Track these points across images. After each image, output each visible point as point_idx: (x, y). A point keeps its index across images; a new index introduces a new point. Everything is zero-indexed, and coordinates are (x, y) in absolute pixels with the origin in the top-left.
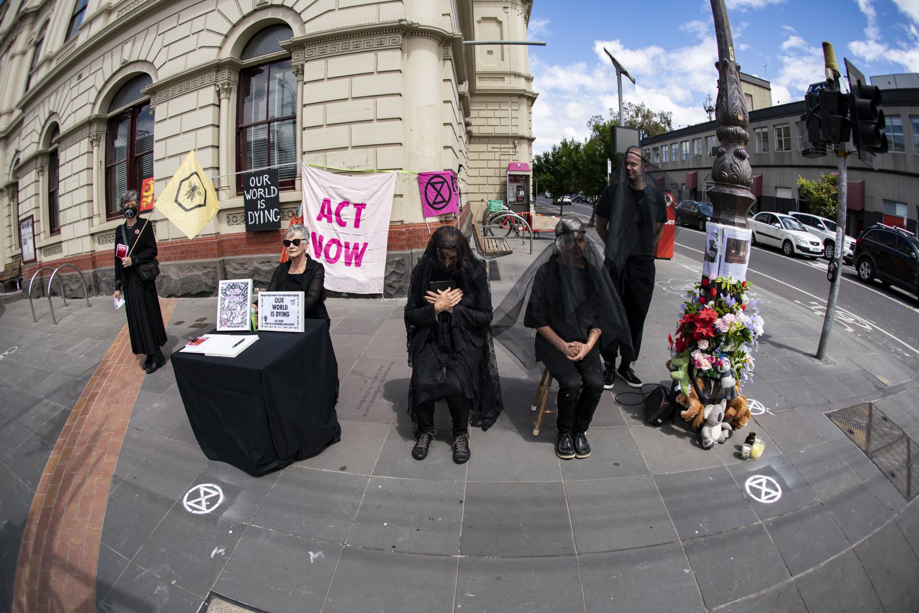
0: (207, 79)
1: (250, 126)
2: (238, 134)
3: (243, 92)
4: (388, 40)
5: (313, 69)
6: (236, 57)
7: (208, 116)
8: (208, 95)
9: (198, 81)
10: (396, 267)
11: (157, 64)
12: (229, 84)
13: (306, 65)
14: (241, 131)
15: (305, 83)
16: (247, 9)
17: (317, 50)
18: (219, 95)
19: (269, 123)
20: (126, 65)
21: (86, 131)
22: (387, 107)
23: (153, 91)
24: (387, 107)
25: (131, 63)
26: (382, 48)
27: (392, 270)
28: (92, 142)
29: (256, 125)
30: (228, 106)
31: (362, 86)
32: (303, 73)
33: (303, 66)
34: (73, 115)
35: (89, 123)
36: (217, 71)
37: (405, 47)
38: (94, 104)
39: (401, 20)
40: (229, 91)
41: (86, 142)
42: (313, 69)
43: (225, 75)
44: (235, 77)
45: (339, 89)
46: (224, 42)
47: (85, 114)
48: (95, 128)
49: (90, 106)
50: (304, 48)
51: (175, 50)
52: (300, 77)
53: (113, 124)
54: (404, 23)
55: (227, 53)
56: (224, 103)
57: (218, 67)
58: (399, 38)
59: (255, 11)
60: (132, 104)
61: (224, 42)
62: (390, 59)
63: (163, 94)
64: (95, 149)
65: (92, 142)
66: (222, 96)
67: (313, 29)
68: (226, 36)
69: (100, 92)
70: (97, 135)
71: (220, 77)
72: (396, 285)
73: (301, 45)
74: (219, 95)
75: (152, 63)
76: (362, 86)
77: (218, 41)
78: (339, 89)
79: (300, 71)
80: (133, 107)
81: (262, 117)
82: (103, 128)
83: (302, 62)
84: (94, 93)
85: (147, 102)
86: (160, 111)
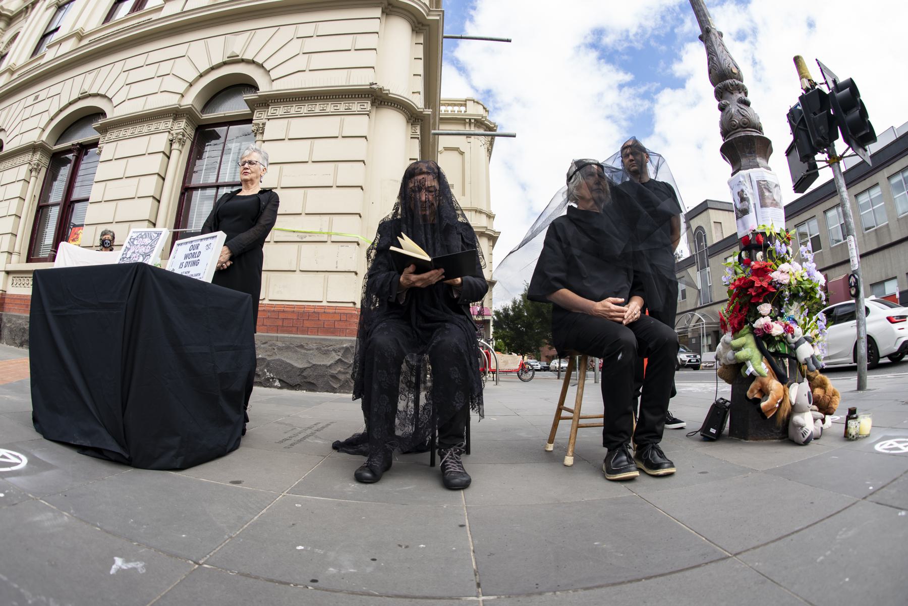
0: (162, 125)
1: (196, 188)
2: (182, 194)
3: (196, 153)
4: (356, 106)
5: (273, 129)
6: (198, 107)
7: (155, 163)
8: (160, 142)
9: (153, 126)
10: (343, 355)
11: (116, 101)
12: (184, 135)
13: (268, 123)
14: (187, 191)
15: (264, 141)
16: (217, 60)
17: (281, 110)
18: (171, 145)
19: (218, 187)
20: (85, 96)
21: (27, 157)
22: (349, 174)
23: (103, 130)
24: (349, 174)
25: (90, 95)
26: (349, 113)
27: (337, 358)
28: (31, 171)
29: (204, 187)
30: (179, 159)
31: (323, 150)
32: (262, 133)
33: (264, 124)
34: (20, 136)
35: (33, 148)
36: (175, 119)
37: (373, 115)
38: (44, 130)
39: (372, 84)
40: (182, 142)
41: (25, 169)
42: (273, 129)
43: (182, 124)
44: (190, 132)
45: (300, 151)
46: (187, 90)
47: (33, 137)
48: (38, 156)
49: (39, 131)
50: (269, 106)
51: (137, 90)
52: (259, 137)
53: (57, 160)
54: (374, 86)
55: (189, 101)
56: (175, 154)
57: (175, 114)
58: (368, 106)
59: (225, 64)
60: (81, 140)
61: (187, 90)
62: (357, 124)
63: (113, 135)
64: (33, 179)
65: (31, 171)
66: (176, 146)
67: (281, 86)
68: (191, 85)
69: (52, 119)
70: (38, 165)
71: (176, 127)
72: (342, 377)
73: (266, 102)
74: (171, 145)
75: (110, 100)
76: (323, 150)
77: (182, 87)
78: (300, 151)
79: (260, 130)
80: (80, 144)
81: (212, 180)
82: (46, 161)
83: (264, 121)
84: (46, 118)
85: (95, 144)
86: (107, 150)
